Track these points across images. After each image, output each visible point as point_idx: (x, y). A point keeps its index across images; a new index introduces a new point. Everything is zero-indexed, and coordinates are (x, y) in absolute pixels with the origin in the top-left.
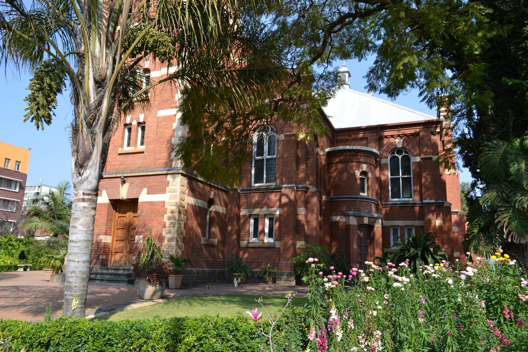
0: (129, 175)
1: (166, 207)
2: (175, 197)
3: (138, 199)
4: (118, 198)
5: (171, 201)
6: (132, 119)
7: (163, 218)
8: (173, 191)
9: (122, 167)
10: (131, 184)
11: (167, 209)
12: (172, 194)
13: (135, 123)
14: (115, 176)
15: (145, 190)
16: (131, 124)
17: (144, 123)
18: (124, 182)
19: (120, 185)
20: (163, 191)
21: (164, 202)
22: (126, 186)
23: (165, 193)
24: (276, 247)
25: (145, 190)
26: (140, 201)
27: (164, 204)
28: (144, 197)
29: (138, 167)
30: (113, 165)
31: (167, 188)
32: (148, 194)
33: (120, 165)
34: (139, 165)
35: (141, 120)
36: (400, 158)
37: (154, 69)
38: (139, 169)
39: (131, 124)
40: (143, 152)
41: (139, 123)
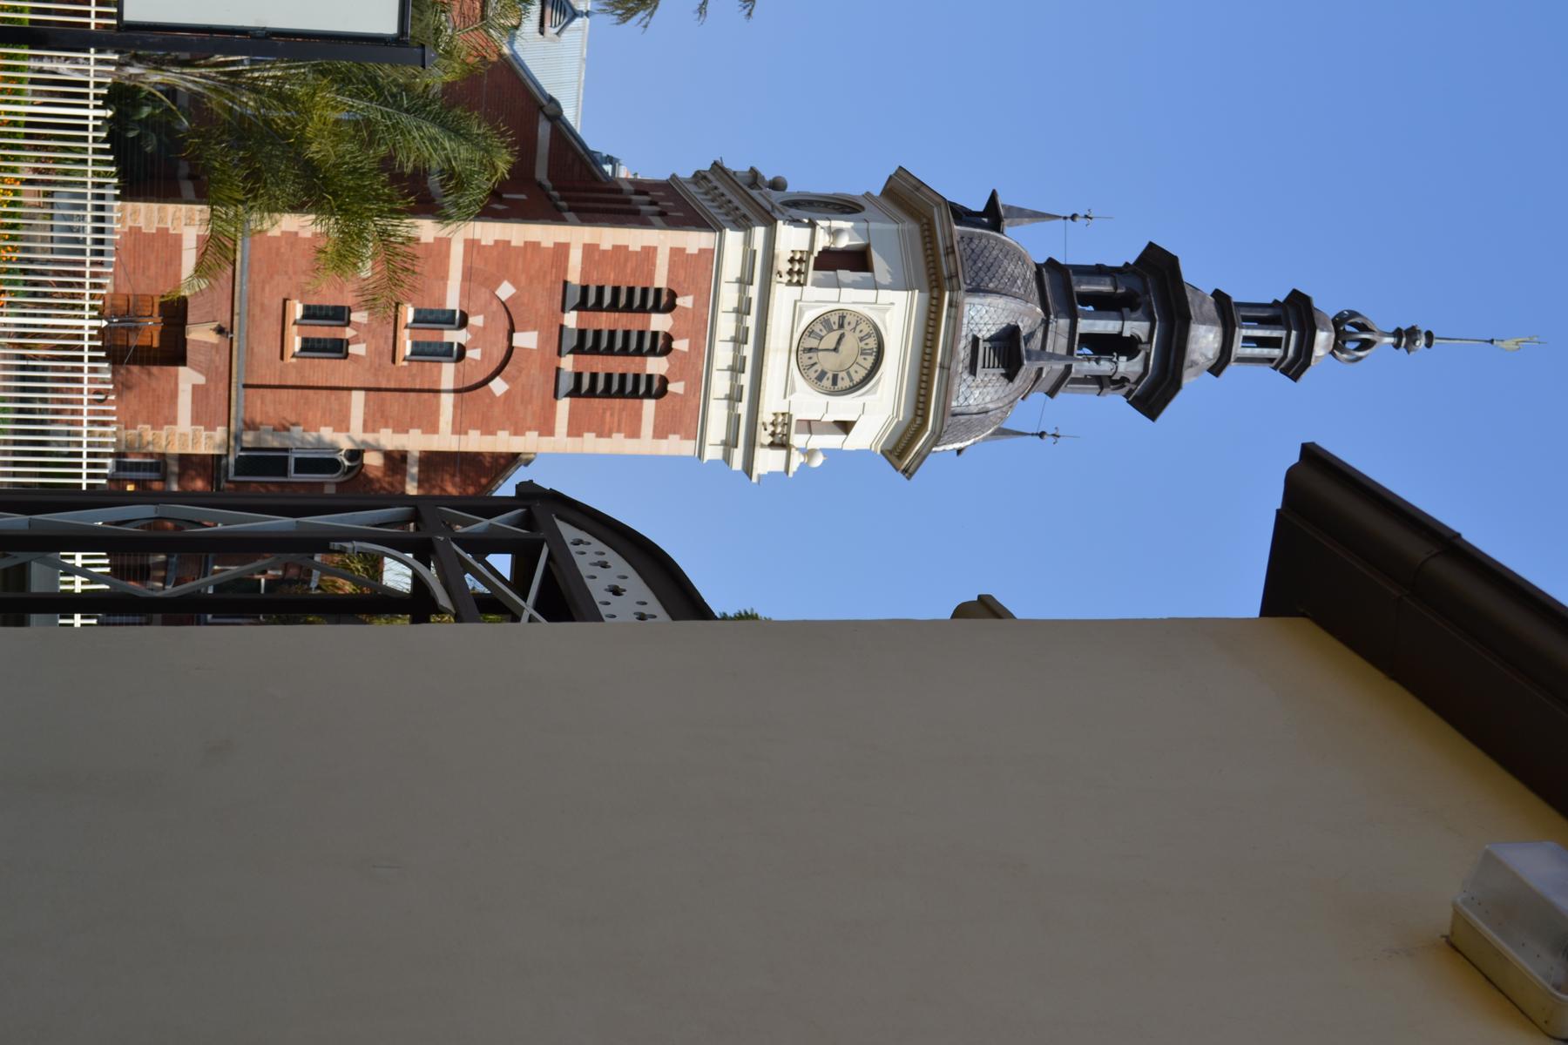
2: (184, 445)
4: (190, 319)
6: (358, 326)
8: (195, 442)
9: (257, 311)
10: (215, 347)
13: (349, 333)
14: (236, 310)
15: (201, 380)
16: (348, 323)
17: (346, 356)
18: (220, 330)
19: (214, 325)
20: (196, 420)
21: (173, 421)
22: (213, 338)
25: (201, 380)
26: (182, 370)
28: (187, 378)
30: (263, 289)
32: (195, 387)
33: (262, 306)
35: (352, 349)
37: (457, 371)
38: (250, 351)
39: (348, 323)
40: (282, 358)
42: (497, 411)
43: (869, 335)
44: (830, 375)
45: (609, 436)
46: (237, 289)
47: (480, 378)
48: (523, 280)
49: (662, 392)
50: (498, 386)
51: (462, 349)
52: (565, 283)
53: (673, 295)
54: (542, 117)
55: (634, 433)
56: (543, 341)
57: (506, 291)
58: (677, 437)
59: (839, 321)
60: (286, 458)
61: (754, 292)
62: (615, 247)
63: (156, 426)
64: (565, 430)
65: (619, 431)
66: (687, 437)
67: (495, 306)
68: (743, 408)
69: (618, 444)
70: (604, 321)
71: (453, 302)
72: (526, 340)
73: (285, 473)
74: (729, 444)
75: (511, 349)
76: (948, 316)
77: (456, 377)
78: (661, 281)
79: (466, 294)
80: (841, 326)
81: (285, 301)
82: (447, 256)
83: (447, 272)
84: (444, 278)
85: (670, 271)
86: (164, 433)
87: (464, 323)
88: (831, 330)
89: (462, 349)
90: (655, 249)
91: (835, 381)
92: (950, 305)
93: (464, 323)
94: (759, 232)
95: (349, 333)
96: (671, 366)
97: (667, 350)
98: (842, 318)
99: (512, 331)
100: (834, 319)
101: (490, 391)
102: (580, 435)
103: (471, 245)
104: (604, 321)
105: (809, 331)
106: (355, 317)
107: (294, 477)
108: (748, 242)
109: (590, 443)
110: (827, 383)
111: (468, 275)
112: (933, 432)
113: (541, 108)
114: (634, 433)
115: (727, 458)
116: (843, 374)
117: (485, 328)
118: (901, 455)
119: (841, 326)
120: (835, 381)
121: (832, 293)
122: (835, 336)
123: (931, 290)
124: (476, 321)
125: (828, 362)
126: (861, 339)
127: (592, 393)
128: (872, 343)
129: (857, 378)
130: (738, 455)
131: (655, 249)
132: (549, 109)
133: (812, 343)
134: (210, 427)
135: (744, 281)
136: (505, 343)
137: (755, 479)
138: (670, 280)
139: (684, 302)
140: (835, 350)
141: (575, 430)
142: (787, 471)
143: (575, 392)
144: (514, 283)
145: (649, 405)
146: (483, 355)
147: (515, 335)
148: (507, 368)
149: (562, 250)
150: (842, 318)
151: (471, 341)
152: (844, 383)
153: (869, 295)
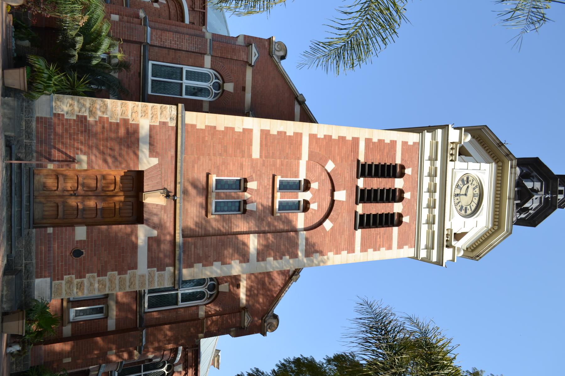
0: (178, 205)
1: (129, 271)
3: (143, 223)
4: (146, 188)
5: (137, 278)
7: (112, 270)
10: (163, 208)
11: (126, 273)
12: (147, 277)
13: (247, 195)
14: (178, 180)
16: (245, 189)
17: (245, 211)
18: (168, 196)
20: (151, 263)
21: (135, 267)
23: (148, 267)
24: (64, 328)
27: (133, 269)
29: (187, 210)
30: (193, 167)
31: (155, 269)
34: (189, 211)
36: (162, 370)
37: (306, 217)
39: (245, 189)
41: (245, 202)
42: (327, 239)
43: (476, 186)
44: (464, 208)
45: (379, 250)
46: (179, 164)
47: (316, 221)
48: (338, 158)
49: (400, 223)
50: (328, 225)
51: (307, 203)
52: (358, 161)
53: (403, 167)
54: (296, 103)
55: (390, 248)
56: (348, 196)
57: (330, 166)
58: (407, 247)
59: (466, 180)
60: (177, 294)
61: (438, 164)
62: (380, 141)
63: (122, 272)
64: (359, 248)
65: (383, 247)
66: (411, 247)
67: (325, 177)
68: (436, 227)
69: (383, 254)
70: (377, 183)
71: (302, 177)
72: (340, 196)
73: (176, 303)
74: (429, 248)
75: (333, 201)
76: (511, 173)
77: (305, 221)
78: (398, 161)
79: (309, 169)
80: (468, 182)
81: (208, 175)
82: (301, 144)
83: (301, 154)
84: (299, 158)
85: (402, 154)
86: (127, 277)
87: (307, 186)
88: (464, 185)
89: (307, 203)
90: (396, 141)
91: (466, 212)
92: (512, 167)
93: (307, 186)
94: (439, 131)
95: (247, 195)
96: (404, 207)
97: (401, 199)
98: (468, 178)
99: (333, 190)
100: (465, 179)
101: (324, 228)
102: (366, 251)
103: (313, 137)
104: (377, 183)
105: (458, 186)
106: (251, 185)
107: (181, 304)
108: (434, 138)
109: (372, 255)
110: (463, 212)
111: (311, 156)
112: (507, 231)
113: (296, 98)
114: (390, 248)
115: (429, 255)
116: (468, 207)
117: (319, 190)
118: (472, 251)
119: (468, 182)
120: (466, 212)
121: (464, 165)
122: (466, 186)
123: (497, 163)
124: (314, 185)
125: (464, 201)
126: (474, 189)
127: (368, 226)
128: (477, 190)
129: (473, 208)
130: (435, 253)
131: (396, 141)
132: (300, 99)
133: (458, 191)
134: (161, 268)
135: (433, 159)
136: (329, 199)
137: (444, 265)
138: (402, 160)
139: (408, 171)
140: (466, 195)
141: (364, 249)
142: (453, 260)
143: (362, 226)
144: (334, 161)
145: (395, 229)
146: (319, 206)
147: (336, 193)
148: (332, 214)
149: (356, 141)
150: (468, 178)
151: (312, 199)
152: (469, 212)
153: (477, 165)
